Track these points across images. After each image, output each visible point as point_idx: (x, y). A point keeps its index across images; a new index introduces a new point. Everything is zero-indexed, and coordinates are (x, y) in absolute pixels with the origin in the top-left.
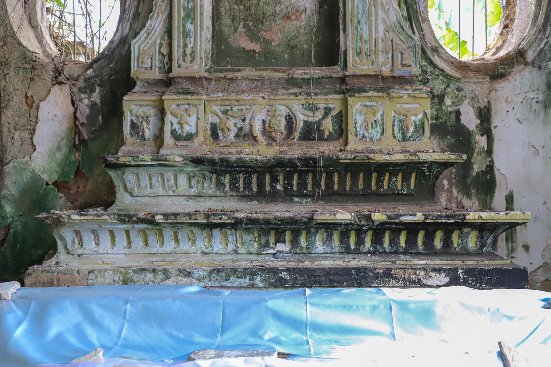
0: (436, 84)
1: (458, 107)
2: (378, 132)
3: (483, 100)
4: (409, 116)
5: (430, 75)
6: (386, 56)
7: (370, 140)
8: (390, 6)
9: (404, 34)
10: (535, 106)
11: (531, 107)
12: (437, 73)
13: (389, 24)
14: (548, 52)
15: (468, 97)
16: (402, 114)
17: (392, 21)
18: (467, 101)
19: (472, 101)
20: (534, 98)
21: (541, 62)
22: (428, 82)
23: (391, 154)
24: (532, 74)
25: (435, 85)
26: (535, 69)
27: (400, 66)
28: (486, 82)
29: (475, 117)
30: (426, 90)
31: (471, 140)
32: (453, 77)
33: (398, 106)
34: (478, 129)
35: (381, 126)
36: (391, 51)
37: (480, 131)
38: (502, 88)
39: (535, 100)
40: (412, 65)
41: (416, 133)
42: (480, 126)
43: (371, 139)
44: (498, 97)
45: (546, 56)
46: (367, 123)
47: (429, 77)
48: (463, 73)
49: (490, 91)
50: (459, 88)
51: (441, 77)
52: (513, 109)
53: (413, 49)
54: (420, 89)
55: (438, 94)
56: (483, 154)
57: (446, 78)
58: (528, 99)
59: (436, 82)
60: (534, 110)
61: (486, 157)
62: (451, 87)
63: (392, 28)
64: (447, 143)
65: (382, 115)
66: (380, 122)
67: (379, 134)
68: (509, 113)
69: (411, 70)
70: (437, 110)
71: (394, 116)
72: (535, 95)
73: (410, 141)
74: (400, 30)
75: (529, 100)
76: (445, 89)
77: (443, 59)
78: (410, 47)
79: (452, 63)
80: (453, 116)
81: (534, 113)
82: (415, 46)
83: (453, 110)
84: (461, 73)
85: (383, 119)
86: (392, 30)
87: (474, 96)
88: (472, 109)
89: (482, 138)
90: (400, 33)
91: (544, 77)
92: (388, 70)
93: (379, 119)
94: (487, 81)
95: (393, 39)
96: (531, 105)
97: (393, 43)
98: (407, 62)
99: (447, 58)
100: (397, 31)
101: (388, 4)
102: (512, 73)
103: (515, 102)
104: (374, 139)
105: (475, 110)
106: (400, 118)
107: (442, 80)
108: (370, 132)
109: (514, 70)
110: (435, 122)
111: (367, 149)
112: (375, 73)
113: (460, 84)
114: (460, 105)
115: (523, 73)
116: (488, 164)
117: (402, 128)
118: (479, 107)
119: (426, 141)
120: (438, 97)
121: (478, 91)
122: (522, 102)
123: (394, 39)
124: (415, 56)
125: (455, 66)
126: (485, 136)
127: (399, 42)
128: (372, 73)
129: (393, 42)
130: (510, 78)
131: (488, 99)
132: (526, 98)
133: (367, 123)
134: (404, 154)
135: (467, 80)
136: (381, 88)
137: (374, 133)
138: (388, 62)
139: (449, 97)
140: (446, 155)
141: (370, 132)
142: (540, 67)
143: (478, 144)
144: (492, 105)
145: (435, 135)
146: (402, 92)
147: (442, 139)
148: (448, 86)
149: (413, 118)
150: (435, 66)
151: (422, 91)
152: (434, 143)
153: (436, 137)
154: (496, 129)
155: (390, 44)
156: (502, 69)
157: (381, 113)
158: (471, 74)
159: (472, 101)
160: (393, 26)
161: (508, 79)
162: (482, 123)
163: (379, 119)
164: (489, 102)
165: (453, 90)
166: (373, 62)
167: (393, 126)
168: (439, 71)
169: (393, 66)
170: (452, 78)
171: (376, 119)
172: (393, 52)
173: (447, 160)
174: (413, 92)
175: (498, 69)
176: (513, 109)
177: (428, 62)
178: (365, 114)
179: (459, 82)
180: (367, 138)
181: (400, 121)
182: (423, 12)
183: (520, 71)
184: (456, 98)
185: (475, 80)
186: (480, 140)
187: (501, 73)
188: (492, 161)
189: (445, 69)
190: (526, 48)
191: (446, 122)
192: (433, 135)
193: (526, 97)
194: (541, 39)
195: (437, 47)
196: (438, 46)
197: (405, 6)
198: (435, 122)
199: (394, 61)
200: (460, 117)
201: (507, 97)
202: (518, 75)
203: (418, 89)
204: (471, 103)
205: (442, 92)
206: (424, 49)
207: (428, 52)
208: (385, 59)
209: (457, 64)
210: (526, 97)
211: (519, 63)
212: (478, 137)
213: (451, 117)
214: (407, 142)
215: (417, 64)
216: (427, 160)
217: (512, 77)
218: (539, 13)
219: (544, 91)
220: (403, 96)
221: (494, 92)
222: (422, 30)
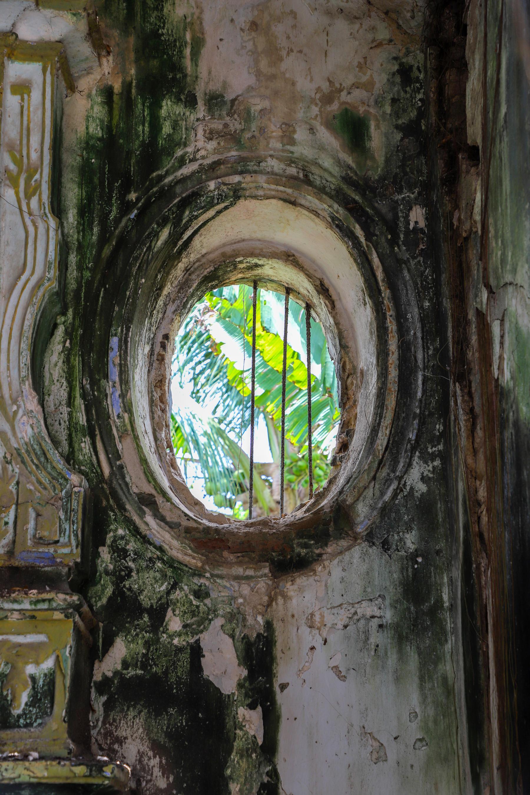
0: (147, 582)
1: (196, 637)
3: (256, 620)
4: (20, 665)
5: (134, 560)
8: (19, 407)
9: (49, 469)
10: (375, 638)
11: (367, 639)
12: (149, 555)
13: (16, 446)
14: (403, 510)
15: (221, 612)
17: (23, 438)
18: (218, 622)
19: (230, 621)
20: (373, 617)
21: (388, 532)
22: (129, 576)
24: (367, 561)
25: (144, 582)
26: (374, 547)
28: (261, 576)
29: (236, 661)
30: (65, 600)
31: (225, 719)
32: (186, 566)
34: (243, 691)
36: (14, 507)
37: (246, 695)
38: (301, 590)
39: (375, 622)
40: (62, 540)
41: (34, 707)
42: (247, 684)
44: (290, 614)
45: (400, 519)
47: (131, 564)
48: (210, 555)
49: (272, 600)
50: (199, 590)
51: (159, 565)
52: (325, 642)
53: (67, 502)
54: (50, 600)
55: (152, 606)
56: (254, 755)
57: (171, 566)
58: (358, 620)
59: (147, 575)
60: (373, 647)
61: (260, 764)
62: (181, 589)
63: (19, 455)
64: (168, 728)
68: (316, 652)
69: (56, 551)
70: (147, 644)
72: (376, 609)
73: (19, 727)
74: (38, 459)
75: (362, 622)
76: (168, 593)
77: (167, 523)
79: (188, 530)
80: (185, 658)
81: (373, 653)
82: (71, 496)
83: (184, 643)
84: (206, 556)
86: (19, 459)
87: (235, 611)
88: (230, 641)
89: (252, 712)
91: (396, 567)
94: (265, 575)
95: (20, 480)
96: (367, 634)
97: (20, 489)
98: (46, 534)
99: (175, 520)
100: (32, 461)
101: (15, 401)
102: (324, 557)
103: (329, 625)
105: (238, 644)
107: (161, 571)
109: (329, 550)
110: (140, 672)
113: (202, 581)
114: (202, 632)
115: (347, 556)
116: (266, 779)
118: (246, 637)
119: (54, 726)
120: (151, 611)
121: (245, 599)
122: (345, 627)
123: (23, 480)
125: (194, 540)
126: (259, 709)
129: (20, 486)
130: (319, 569)
131: (268, 617)
132: (356, 617)
135: (219, 572)
138: (6, 532)
139: (177, 612)
140: (64, 765)
142: (386, 546)
143: (241, 729)
144: (276, 634)
145: (138, 706)
146: (7, 606)
147: (156, 716)
148: (174, 586)
149: (30, 669)
150: (145, 540)
152: (135, 727)
153: (140, 712)
154: (285, 691)
155: (14, 491)
156: (302, 548)
158: (231, 557)
159: (230, 621)
160: (23, 451)
161: (314, 571)
162: (251, 677)
164: (269, 625)
165: (186, 596)
168: (154, 550)
170: (184, 568)
172: (17, 510)
173: (67, 778)
174: (33, 607)
175: (293, 548)
176: (325, 642)
177: (129, 530)
179: (201, 576)
182: (119, 417)
183: (341, 553)
184: (193, 614)
185: (239, 571)
186: (247, 717)
187: (299, 555)
188: (274, 774)
189: (166, 547)
190: (349, 501)
191: (166, 673)
192: (135, 708)
193: (356, 613)
194: (388, 481)
195: (151, 495)
196: (154, 492)
197: (82, 402)
198: (140, 672)
200: (200, 662)
202: (335, 562)
203: (44, 601)
204: (228, 627)
205: (160, 599)
206: (121, 500)
207: (128, 507)
209: (197, 535)
210: (356, 613)
211: (340, 534)
212: (242, 712)
213: (179, 661)
214: (8, 732)
215: (72, 538)
216: (17, 781)
217: (324, 567)
218: (379, 424)
219: (397, 601)
221: (280, 600)
222: (119, 457)
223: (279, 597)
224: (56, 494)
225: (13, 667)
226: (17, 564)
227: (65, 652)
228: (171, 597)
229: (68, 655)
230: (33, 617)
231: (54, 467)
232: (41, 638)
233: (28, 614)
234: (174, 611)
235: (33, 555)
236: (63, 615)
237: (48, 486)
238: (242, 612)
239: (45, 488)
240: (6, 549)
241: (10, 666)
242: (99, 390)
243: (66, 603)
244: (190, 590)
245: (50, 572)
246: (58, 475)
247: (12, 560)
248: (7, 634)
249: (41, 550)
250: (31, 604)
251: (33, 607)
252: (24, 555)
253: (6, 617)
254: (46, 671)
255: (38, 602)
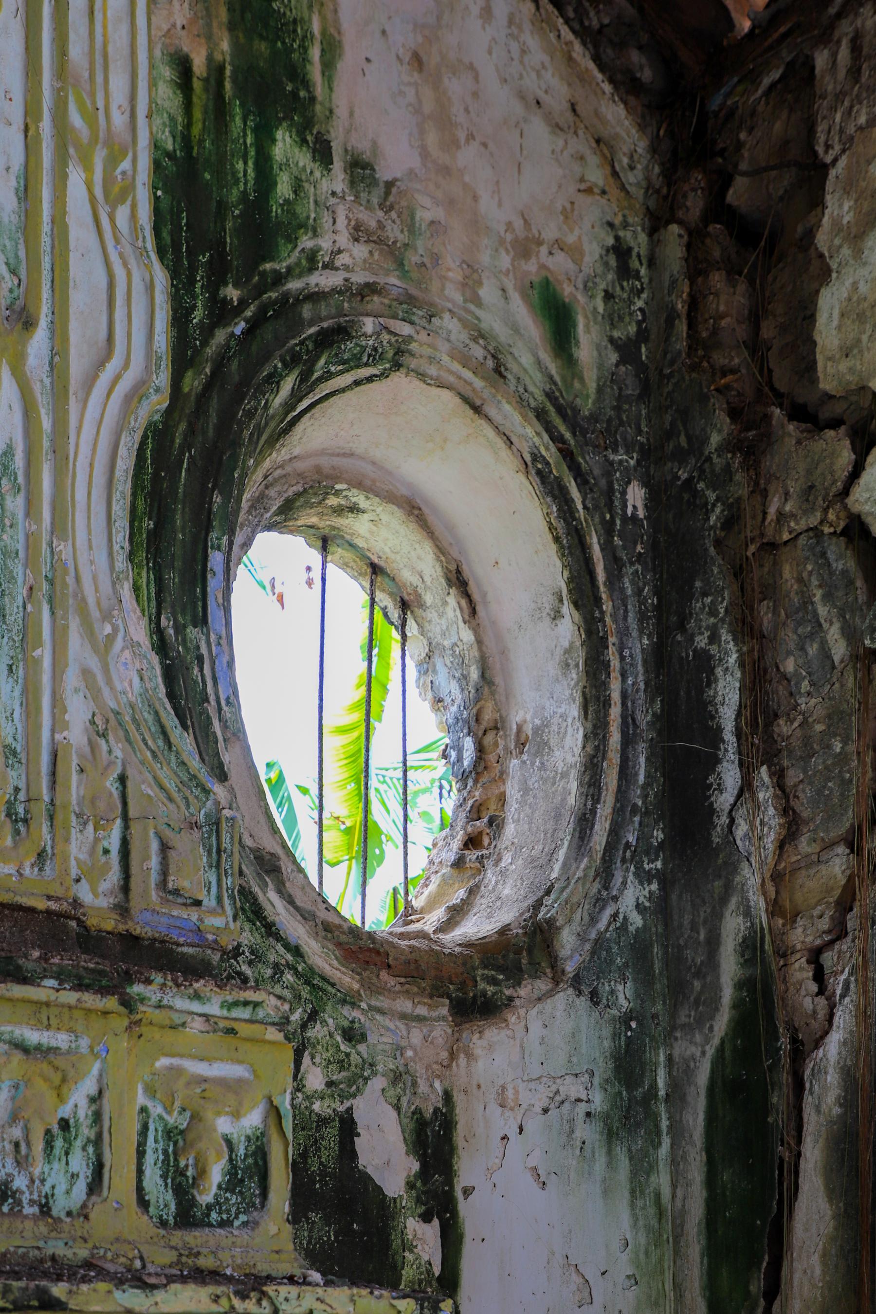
2: (74, 1176)
4: (209, 1115)
6: (97, 840)
7: (36, 1209)
9: (173, 765)
16: (177, 1104)
23: (154, 1287)
27: (154, 895)
33: (163, 1062)
35: (91, 1149)
36: (118, 821)
43: (41, 1206)
46: (27, 1130)
54: (256, 1005)
65: (93, 1100)
66: (86, 1132)
67: (80, 1188)
71: (143, 1110)
78: (196, 825)
85: (97, 1117)
87: (401, 1068)
90: (153, 752)
92: (104, 902)
93: (81, 1114)
104: (59, 1208)
106: (171, 1120)
108: (37, 1172)
111: (24, 1256)
112: (53, 906)
117: (177, 1165)
124: (218, 866)
127: (150, 791)
128: (41, 904)
133: (27, 1130)
134: (211, 1289)
136: (93, 971)
137: (57, 1178)
138: (107, 867)
141: (37, 1172)
146: (180, 1003)
149: (224, 1125)
151: (261, 1014)
155: (116, 794)
157: (89, 1086)
163: (81, 1114)
166: (41, 855)
167: (141, 1154)
169: (125, 888)
171: (65, 1111)
174: (225, 1013)
178: (16, 1087)
180: (25, 1202)
181: (170, 1133)
199: (134, 869)
201: (503, 1088)
203: (246, 1003)
208: (92, 852)
220: (184, 1024)
223: (462, 1055)
224: (192, 815)
225: (196, 1117)
226: (138, 931)
227: (284, 1102)
228: (309, 1034)
229: (289, 1107)
230: (231, 1031)
231: (183, 763)
232: (235, 1071)
233: (222, 1024)
234: (313, 1057)
235: (164, 920)
236: (282, 1034)
237: (175, 795)
238: (412, 1071)
239: (171, 799)
240: (111, 900)
241: (188, 1114)
242: (184, 641)
243: (280, 1014)
244: (337, 1025)
245: (192, 956)
246: (190, 780)
247: (130, 923)
248: (181, 1056)
249: (175, 913)
250: (222, 1007)
251: (225, 1013)
252: (147, 916)
253: (184, 1024)
254: (249, 1132)
255: (236, 1004)
